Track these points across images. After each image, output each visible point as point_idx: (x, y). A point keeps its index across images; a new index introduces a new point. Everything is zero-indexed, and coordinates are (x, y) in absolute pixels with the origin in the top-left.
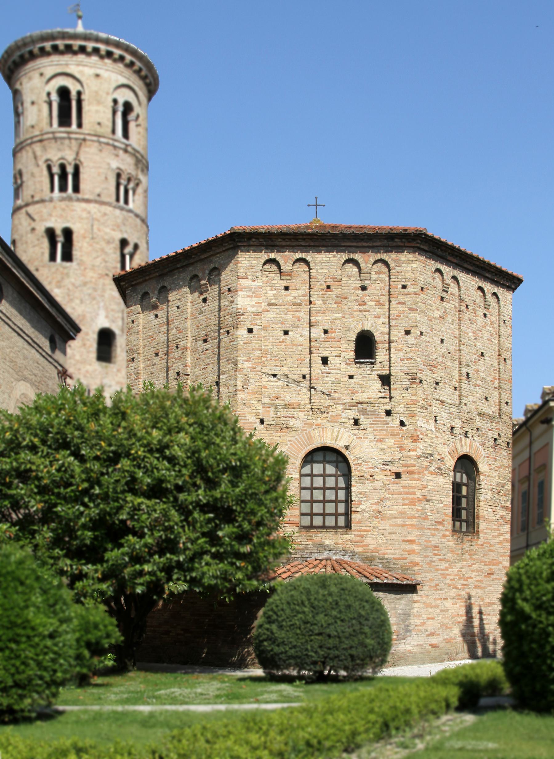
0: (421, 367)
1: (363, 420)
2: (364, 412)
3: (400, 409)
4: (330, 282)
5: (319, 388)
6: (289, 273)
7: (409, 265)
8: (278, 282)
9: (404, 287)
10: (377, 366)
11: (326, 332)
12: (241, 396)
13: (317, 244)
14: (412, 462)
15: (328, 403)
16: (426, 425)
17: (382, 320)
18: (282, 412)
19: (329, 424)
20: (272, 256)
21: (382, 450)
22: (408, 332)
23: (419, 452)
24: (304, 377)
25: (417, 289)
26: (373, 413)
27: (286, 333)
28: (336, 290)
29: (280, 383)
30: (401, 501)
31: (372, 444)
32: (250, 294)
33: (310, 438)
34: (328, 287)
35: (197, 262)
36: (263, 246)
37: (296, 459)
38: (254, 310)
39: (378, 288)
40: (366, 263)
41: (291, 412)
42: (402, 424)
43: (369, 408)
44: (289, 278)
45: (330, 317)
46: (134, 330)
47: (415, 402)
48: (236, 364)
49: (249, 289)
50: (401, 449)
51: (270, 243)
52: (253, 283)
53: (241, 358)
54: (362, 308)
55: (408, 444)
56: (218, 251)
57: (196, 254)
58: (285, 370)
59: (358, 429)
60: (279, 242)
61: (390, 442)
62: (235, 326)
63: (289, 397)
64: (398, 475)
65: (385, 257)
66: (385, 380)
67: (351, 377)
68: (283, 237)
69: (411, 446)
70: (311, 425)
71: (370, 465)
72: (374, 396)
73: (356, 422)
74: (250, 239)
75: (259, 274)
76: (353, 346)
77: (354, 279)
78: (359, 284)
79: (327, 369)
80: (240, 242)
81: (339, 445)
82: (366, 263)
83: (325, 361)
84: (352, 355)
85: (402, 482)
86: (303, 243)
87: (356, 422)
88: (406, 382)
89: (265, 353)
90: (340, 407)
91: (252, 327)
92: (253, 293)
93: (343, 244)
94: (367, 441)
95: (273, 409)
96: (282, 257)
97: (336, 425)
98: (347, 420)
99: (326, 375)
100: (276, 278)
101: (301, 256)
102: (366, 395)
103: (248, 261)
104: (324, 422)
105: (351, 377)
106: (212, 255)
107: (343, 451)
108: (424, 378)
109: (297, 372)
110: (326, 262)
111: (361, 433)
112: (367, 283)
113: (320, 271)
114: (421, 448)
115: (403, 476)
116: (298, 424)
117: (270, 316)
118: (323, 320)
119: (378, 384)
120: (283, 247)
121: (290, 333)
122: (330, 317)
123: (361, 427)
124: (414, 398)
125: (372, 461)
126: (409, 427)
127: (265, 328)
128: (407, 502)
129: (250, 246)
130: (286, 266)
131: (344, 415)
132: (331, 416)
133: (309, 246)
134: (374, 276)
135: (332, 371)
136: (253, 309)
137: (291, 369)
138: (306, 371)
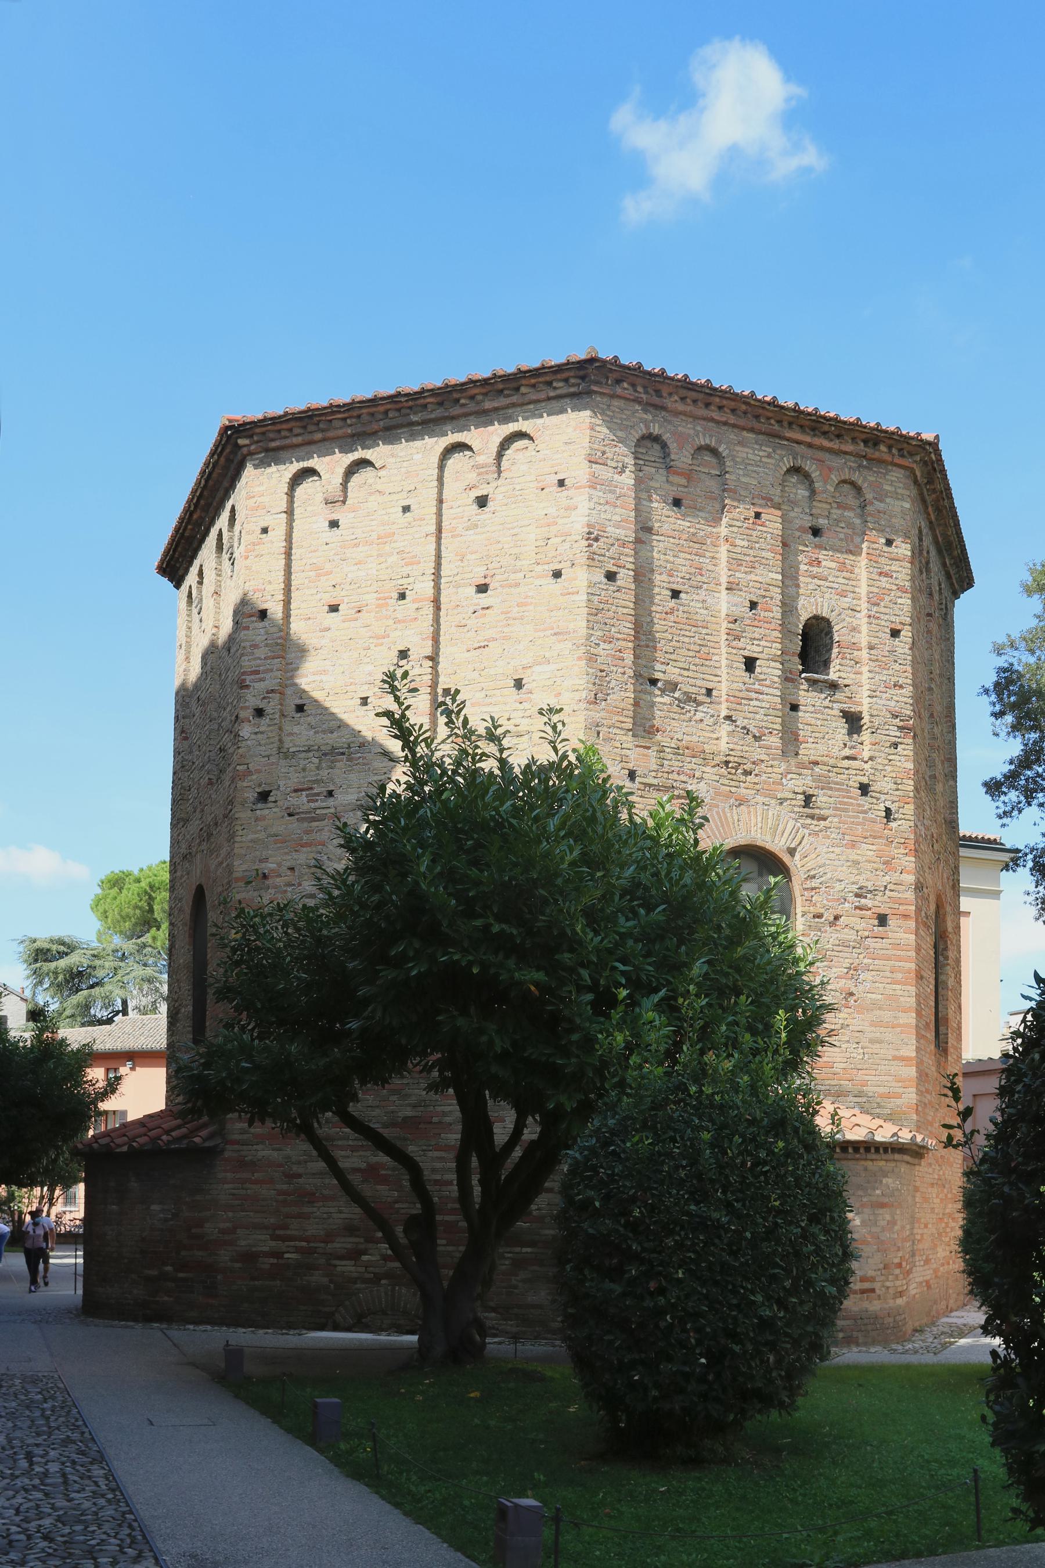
1: (822, 799)
7: (897, 503)
13: (741, 422)
15: (758, 754)
19: (760, 799)
20: (656, 430)
21: (856, 863)
24: (709, 692)
30: (888, 974)
31: (837, 850)
32: (611, 497)
35: (466, 415)
36: (640, 403)
39: (842, 536)
40: (826, 482)
44: (684, 481)
49: (609, 486)
51: (656, 400)
56: (533, 397)
57: (472, 398)
59: (812, 817)
60: (673, 402)
64: (882, 920)
65: (856, 477)
68: (684, 393)
73: (808, 799)
74: (618, 382)
77: (800, 510)
80: (597, 383)
81: (777, 845)
82: (826, 482)
83: (750, 664)
85: (890, 934)
86: (716, 415)
87: (808, 799)
91: (614, 569)
93: (787, 435)
96: (674, 434)
97: (773, 801)
98: (791, 796)
99: (754, 695)
100: (657, 477)
101: (708, 442)
106: (514, 405)
112: (822, 522)
113: (743, 479)
115: (892, 922)
120: (677, 413)
121: (682, 595)
125: (839, 887)
128: (899, 976)
129: (613, 396)
130: (682, 458)
132: (765, 782)
133: (725, 424)
135: (766, 690)
136: (618, 531)
137: (686, 673)
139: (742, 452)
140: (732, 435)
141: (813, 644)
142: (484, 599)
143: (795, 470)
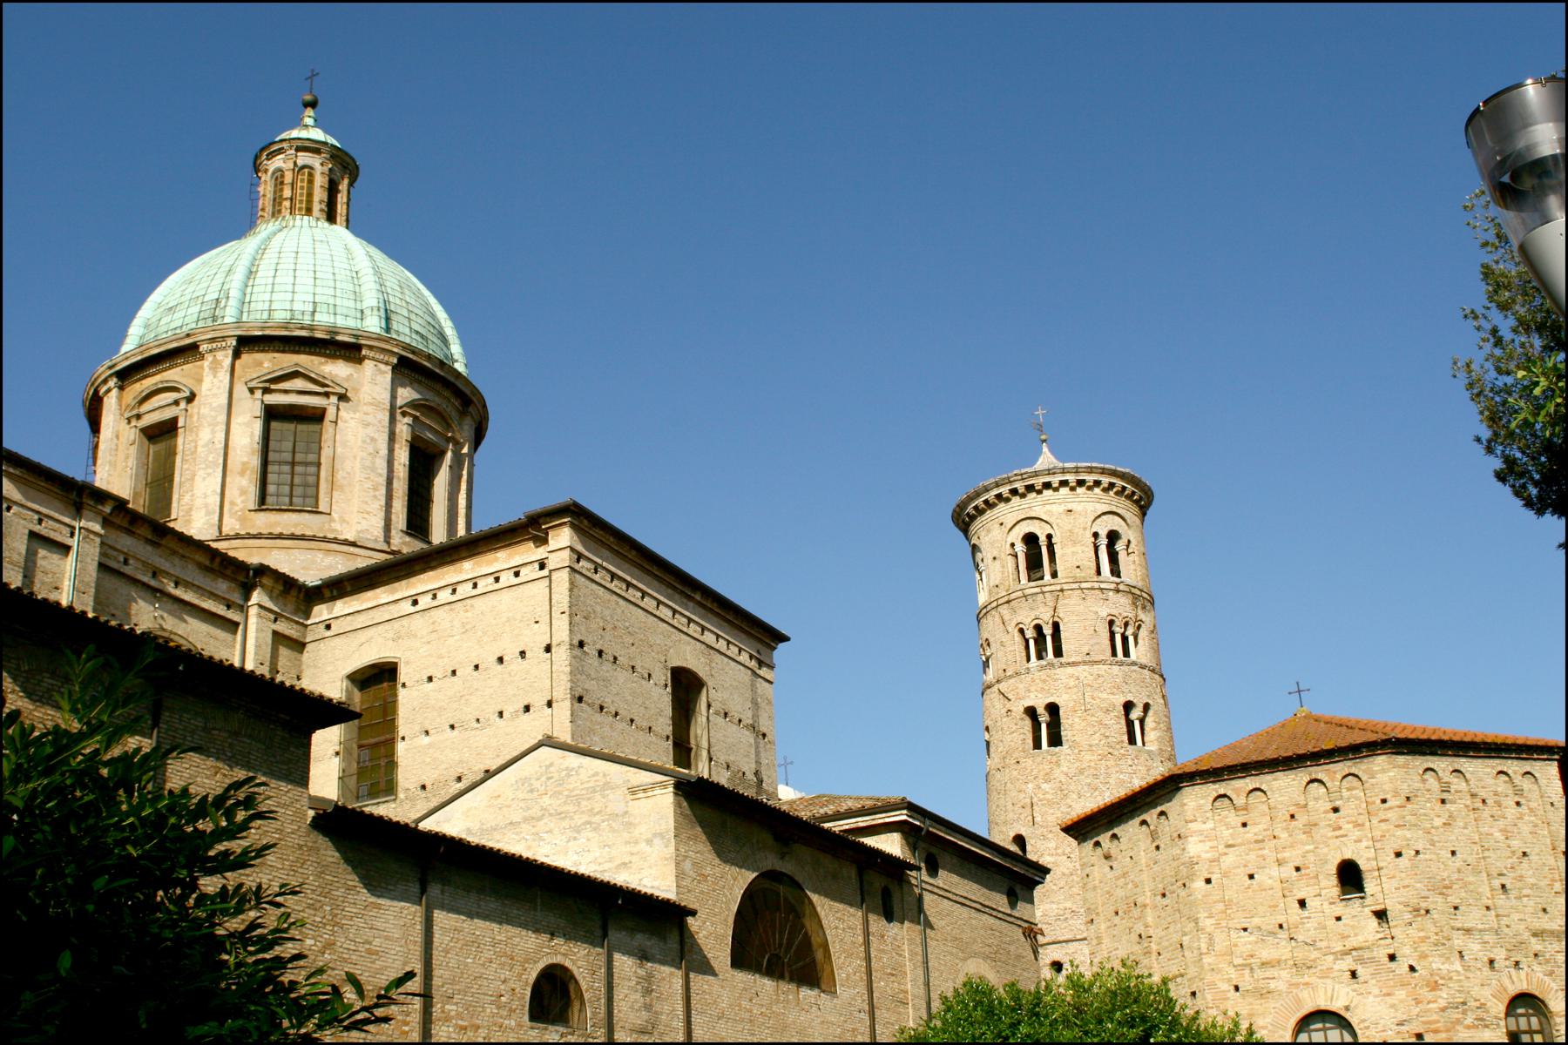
0: (1426, 893)
2: (1360, 960)
3: (1407, 950)
4: (1293, 810)
5: (1300, 938)
6: (1245, 808)
8: (1234, 819)
9: (1384, 801)
10: (1368, 901)
11: (1298, 869)
12: (1207, 960)
14: (1435, 1017)
15: (1314, 955)
16: (1446, 966)
17: (1365, 844)
18: (1259, 974)
20: (1222, 792)
21: (1393, 1006)
22: (1398, 855)
23: (1442, 1003)
24: (1281, 926)
25: (1402, 800)
26: (1373, 960)
27: (1251, 877)
28: (1302, 819)
29: (1252, 938)
33: (1298, 1001)
34: (1292, 816)
37: (1285, 1029)
38: (1209, 855)
41: (1270, 972)
42: (1412, 969)
43: (1367, 954)
45: (1298, 851)
46: (1090, 886)
47: (1423, 940)
48: (1196, 921)
49: (1201, 832)
50: (1418, 1002)
52: (1204, 827)
53: (1202, 915)
54: (1338, 833)
55: (1425, 993)
58: (1256, 921)
61: (1401, 994)
62: (1191, 877)
63: (1266, 954)
66: (1381, 915)
67: (1338, 919)
69: (1430, 996)
70: (1297, 985)
71: (1380, 1028)
72: (1371, 938)
73: (1354, 974)
75: (1209, 814)
76: (1334, 880)
78: (1329, 806)
79: (1305, 913)
81: (1336, 1006)
83: (1302, 903)
84: (1336, 891)
87: (1354, 974)
88: (1408, 917)
89: (1228, 904)
90: (1331, 958)
92: (1206, 837)
94: (1371, 998)
95: (1247, 971)
97: (1329, 981)
102: (1361, 938)
103: (1194, 799)
104: (1313, 980)
105: (1338, 919)
107: (1342, 1013)
108: (1431, 907)
109: (1271, 922)
110: (1284, 786)
111: (1362, 988)
112: (1338, 803)
114: (1444, 996)
116: (1282, 986)
117: (1230, 860)
118: (1294, 856)
119: (1374, 922)
122: (1298, 851)
123: (1361, 979)
124: (1422, 934)
126: (1422, 971)
127: (1225, 875)
130: (1240, 801)
131: (1336, 967)
134: (1345, 794)
138: (1281, 919)
139: (1276, 784)
140: (1269, 777)
141: (1350, 877)
142: (1165, 901)
143: (1312, 781)
